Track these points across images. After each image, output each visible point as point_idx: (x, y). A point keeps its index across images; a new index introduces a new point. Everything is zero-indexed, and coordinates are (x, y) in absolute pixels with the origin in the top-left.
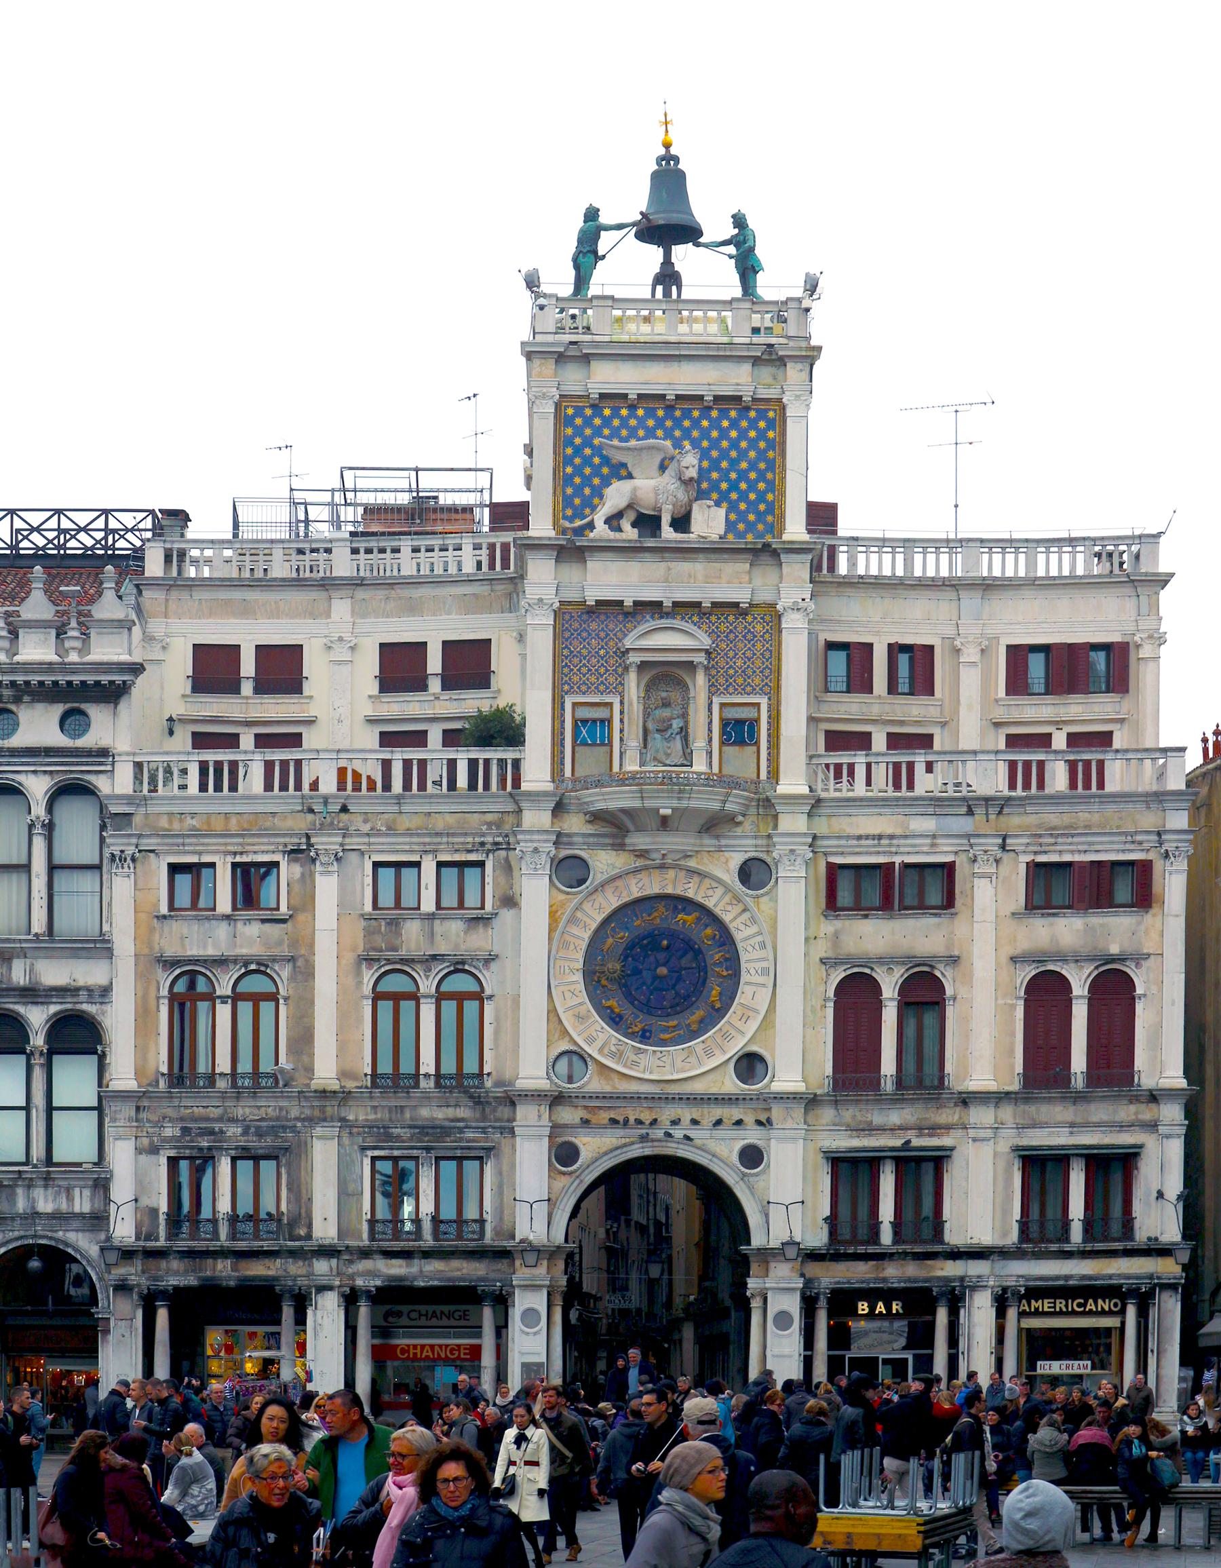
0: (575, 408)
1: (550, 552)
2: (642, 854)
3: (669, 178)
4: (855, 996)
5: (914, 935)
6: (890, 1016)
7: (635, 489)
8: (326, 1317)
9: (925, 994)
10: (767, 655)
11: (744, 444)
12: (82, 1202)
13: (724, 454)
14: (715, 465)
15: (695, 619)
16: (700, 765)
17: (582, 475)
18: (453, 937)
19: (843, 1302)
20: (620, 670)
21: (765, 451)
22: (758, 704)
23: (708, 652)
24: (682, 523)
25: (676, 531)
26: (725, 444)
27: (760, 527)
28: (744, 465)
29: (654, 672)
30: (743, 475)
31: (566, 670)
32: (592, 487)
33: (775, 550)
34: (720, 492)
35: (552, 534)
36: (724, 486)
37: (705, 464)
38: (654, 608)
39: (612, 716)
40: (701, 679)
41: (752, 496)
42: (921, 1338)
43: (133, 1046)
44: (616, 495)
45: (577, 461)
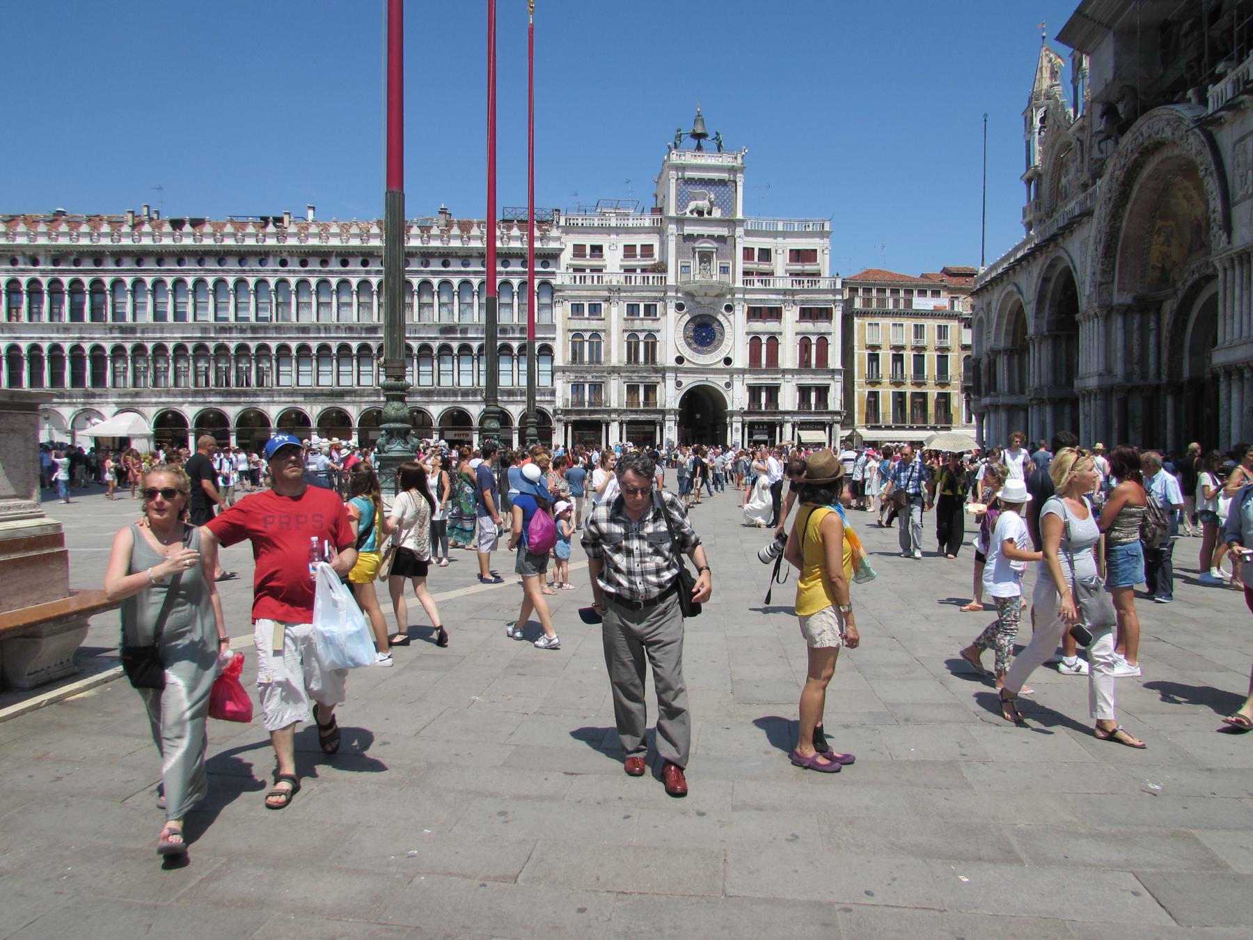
2: (699, 303)
3: (699, 119)
4: (755, 342)
5: (771, 326)
6: (764, 348)
8: (614, 429)
9: (773, 340)
12: (548, 398)
16: (714, 278)
18: (649, 325)
19: (752, 425)
24: (710, 213)
38: (703, 236)
42: (772, 434)
43: (562, 355)
44: (692, 205)
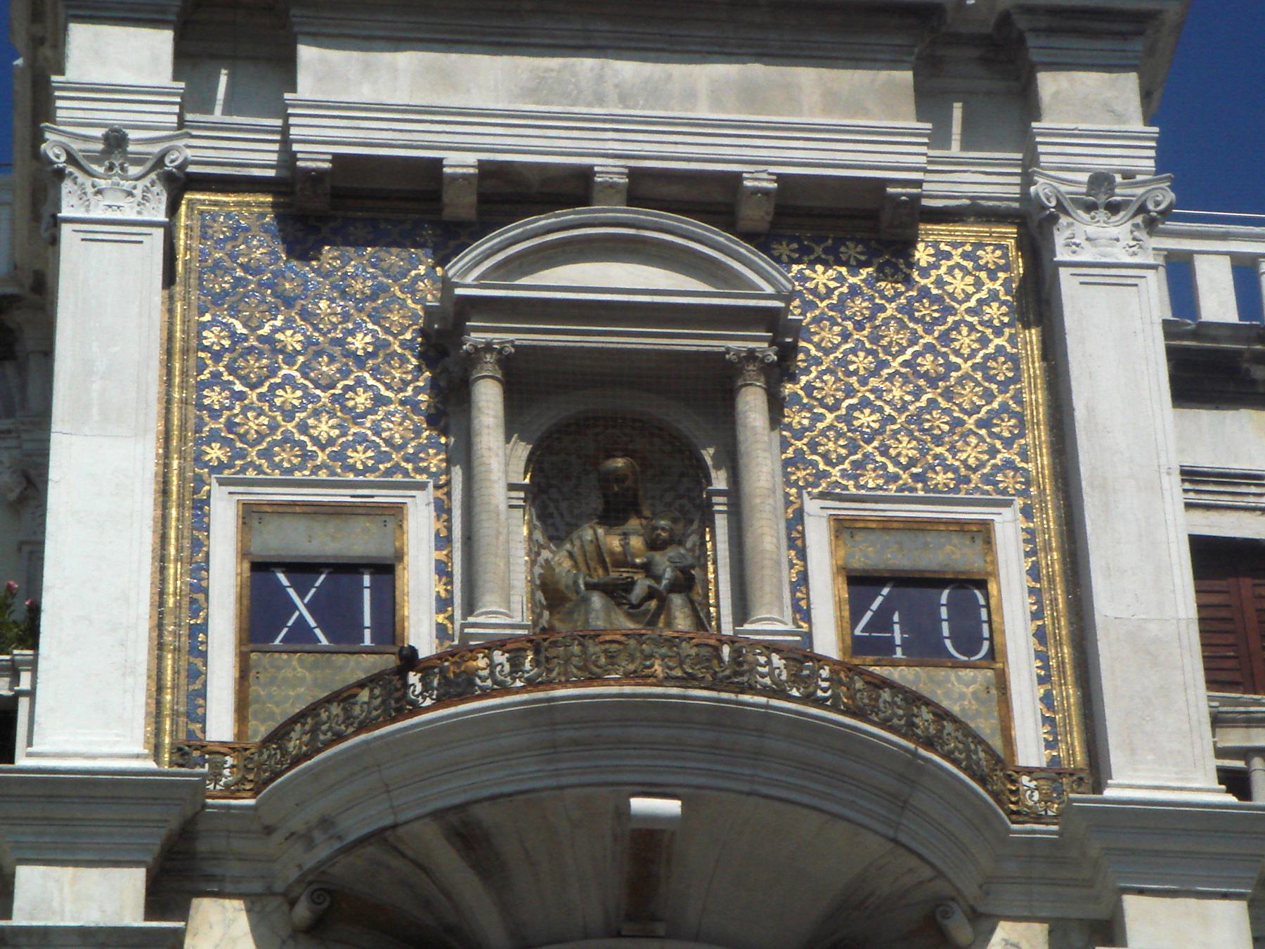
22: (983, 532)
23: (771, 321)
31: (214, 397)
33: (1005, 19)
39: (400, 556)
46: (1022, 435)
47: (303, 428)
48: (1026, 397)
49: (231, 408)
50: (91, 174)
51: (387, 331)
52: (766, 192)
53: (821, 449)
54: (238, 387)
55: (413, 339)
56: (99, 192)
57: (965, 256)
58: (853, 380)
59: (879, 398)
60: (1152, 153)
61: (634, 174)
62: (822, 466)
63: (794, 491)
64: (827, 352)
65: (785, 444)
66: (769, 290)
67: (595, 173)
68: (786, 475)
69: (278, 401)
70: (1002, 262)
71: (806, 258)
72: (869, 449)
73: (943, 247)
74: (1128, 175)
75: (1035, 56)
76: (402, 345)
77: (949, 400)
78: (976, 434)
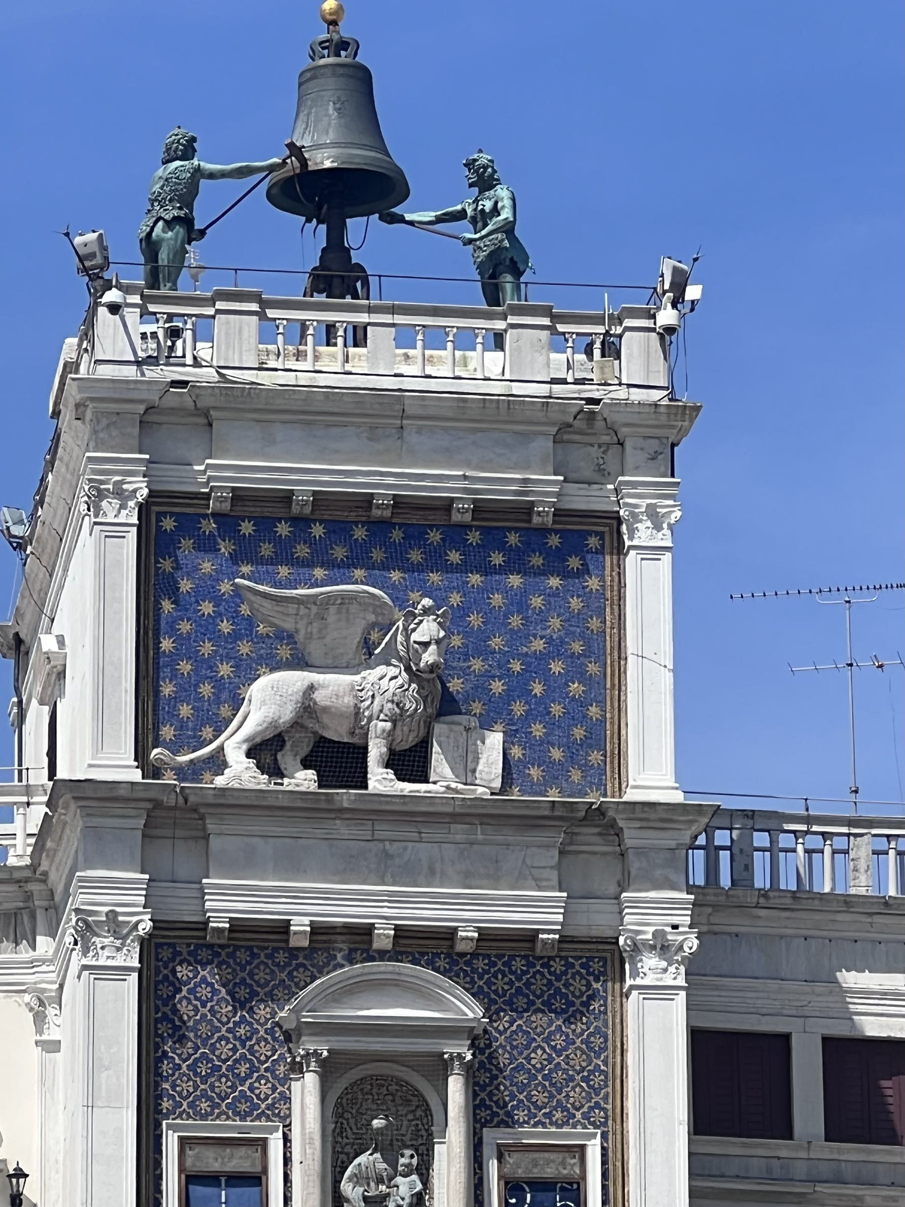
0: (178, 516)
1: (134, 812)
7: (311, 688)
10: (598, 1041)
11: (537, 602)
13: (495, 620)
14: (477, 646)
15: (441, 963)
17: (193, 656)
20: (281, 1069)
21: (580, 618)
25: (400, 779)
26: (497, 599)
27: (576, 775)
28: (538, 645)
29: (354, 1075)
30: (537, 665)
32: (218, 684)
34: (489, 699)
35: (136, 776)
36: (498, 687)
37: (456, 641)
39: (265, 1170)
40: (456, 1087)
41: (557, 709)
45: (185, 627)
46: (607, 1086)
47: (212, 1087)
48: (610, 1060)
49: (173, 1075)
50: (98, 936)
51: (258, 1021)
52: (472, 939)
53: (495, 1099)
54: (177, 1061)
55: (273, 1028)
56: (103, 948)
57: (582, 966)
58: (515, 1052)
59: (529, 1064)
60: (689, 912)
61: (397, 928)
62: (495, 1109)
63: (478, 1126)
64: (501, 1033)
65: (475, 1095)
66: (471, 1015)
67: (375, 928)
68: (475, 1115)
69: (199, 1070)
70: (602, 969)
71: (492, 970)
72: (521, 1097)
73: (570, 960)
74: (675, 927)
75: (629, 842)
76: (266, 1032)
77: (567, 1064)
78: (581, 1087)
